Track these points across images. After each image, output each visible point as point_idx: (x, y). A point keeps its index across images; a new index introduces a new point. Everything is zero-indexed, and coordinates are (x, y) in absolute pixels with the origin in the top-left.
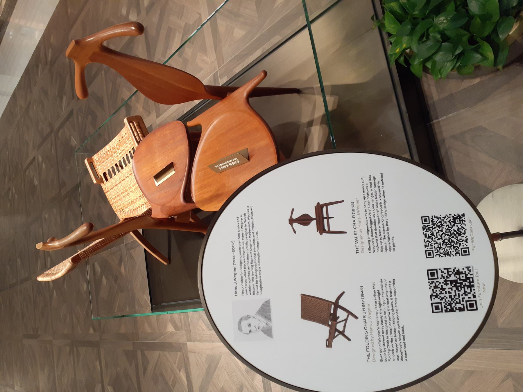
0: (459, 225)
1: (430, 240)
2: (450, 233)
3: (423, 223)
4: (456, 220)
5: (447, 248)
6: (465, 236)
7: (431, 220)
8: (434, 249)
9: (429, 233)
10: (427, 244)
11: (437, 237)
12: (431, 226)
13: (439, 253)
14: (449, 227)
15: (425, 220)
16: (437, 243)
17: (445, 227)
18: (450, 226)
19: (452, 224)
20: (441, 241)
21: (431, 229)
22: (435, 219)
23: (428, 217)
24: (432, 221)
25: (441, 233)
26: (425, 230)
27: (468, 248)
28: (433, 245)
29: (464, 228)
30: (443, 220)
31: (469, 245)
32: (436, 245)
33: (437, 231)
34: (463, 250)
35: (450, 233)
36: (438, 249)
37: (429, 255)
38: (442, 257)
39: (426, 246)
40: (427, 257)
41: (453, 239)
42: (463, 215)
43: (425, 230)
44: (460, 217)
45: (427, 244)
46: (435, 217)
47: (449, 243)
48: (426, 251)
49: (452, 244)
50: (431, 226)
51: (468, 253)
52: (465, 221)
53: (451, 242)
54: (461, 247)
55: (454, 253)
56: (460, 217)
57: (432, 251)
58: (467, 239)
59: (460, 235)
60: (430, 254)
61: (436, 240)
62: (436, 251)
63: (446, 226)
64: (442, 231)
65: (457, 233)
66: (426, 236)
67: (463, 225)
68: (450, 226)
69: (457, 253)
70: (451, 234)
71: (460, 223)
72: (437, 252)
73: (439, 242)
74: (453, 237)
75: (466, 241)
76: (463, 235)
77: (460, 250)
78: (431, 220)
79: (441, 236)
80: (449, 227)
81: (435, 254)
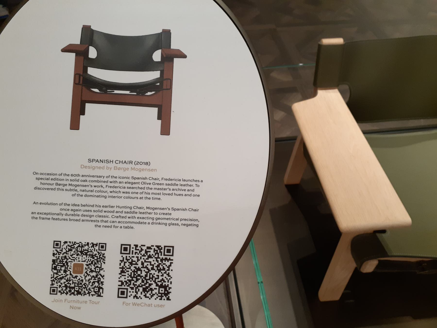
0: (157, 291)
1: (143, 252)
2: (148, 278)
3: (165, 247)
4: (163, 289)
5: (130, 271)
6: (142, 296)
7: (168, 257)
8: (131, 255)
9: (152, 252)
10: (138, 248)
11: (145, 262)
12: (161, 257)
13: (125, 261)
14: (156, 279)
15: (169, 251)
16: (138, 260)
17: (157, 273)
18: (157, 280)
19: (159, 284)
20: (140, 265)
21: (157, 256)
22: (168, 263)
23: (172, 255)
24: (166, 259)
25: (150, 267)
26: (156, 249)
27: (126, 297)
28: (137, 255)
29: (151, 297)
30: (165, 273)
31: (130, 300)
32: (135, 259)
33: (153, 263)
34: (125, 290)
35: (148, 278)
36: (130, 261)
37: (125, 248)
38: (120, 265)
39: (136, 246)
40: (122, 245)
41: (140, 281)
42: (168, 299)
43: (156, 249)
44: (166, 295)
45: (138, 248)
46: (171, 263)
47: (135, 276)
48: (130, 245)
49: (135, 279)
50: (161, 257)
51: (120, 296)
52: (161, 299)
53: (136, 278)
54: (129, 289)
55: (122, 279)
56: (166, 295)
57: (129, 254)
58: (137, 298)
59: (144, 290)
60: (125, 249)
61: (142, 260)
62: (128, 258)
63: (158, 276)
64: (153, 269)
65: (147, 287)
66: (148, 248)
67: (155, 296)
68: (157, 280)
69: (122, 283)
70: (147, 280)
71: (159, 293)
72: (126, 259)
73: (139, 263)
74: (143, 281)
75: (135, 297)
76: (143, 294)
77: (126, 287)
78: (168, 257)
79: (146, 267)
80: (156, 279)
81: (124, 256)
